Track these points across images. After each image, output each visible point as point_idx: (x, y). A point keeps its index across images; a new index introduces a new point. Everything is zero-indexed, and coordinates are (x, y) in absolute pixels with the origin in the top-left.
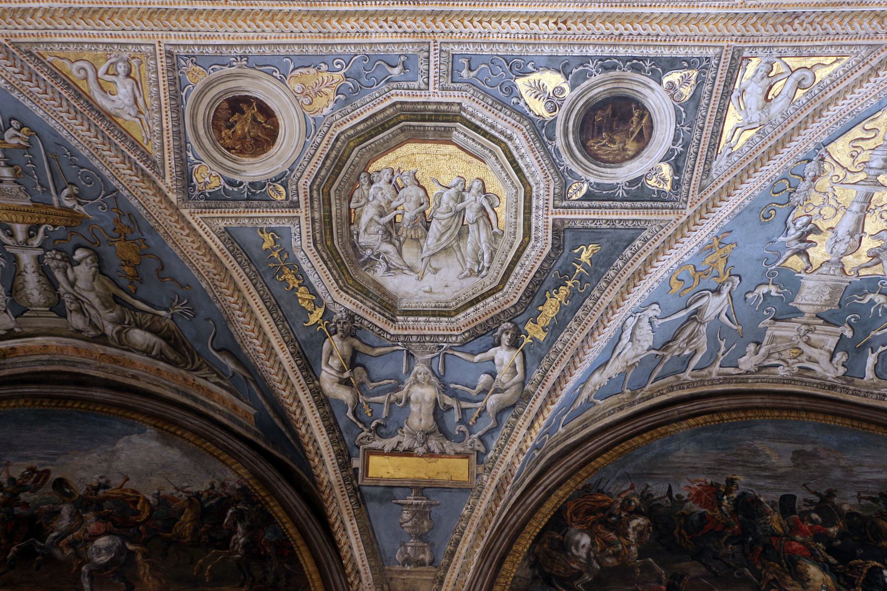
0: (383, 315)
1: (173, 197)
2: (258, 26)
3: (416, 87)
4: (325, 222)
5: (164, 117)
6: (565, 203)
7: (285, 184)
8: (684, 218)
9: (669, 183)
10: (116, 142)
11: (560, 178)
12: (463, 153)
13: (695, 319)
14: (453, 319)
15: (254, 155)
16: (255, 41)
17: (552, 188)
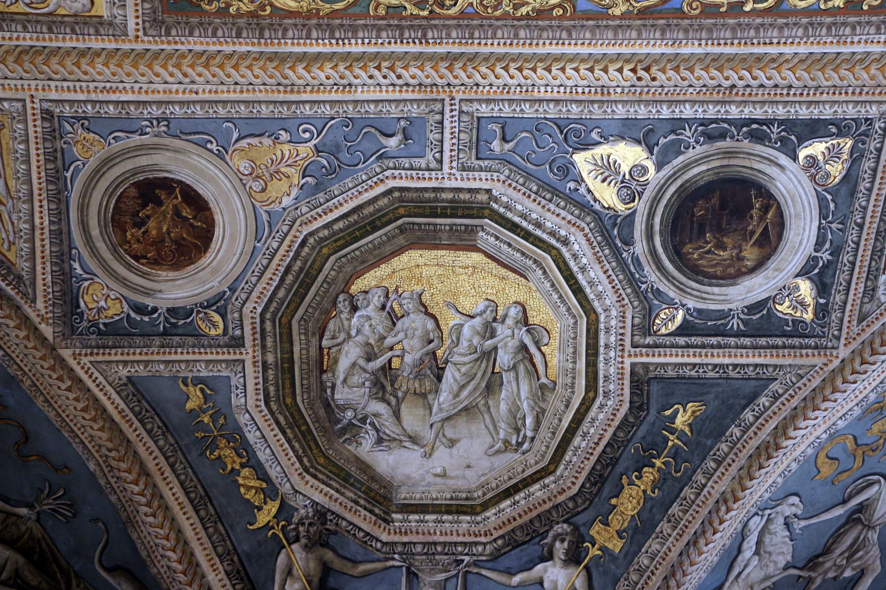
0: (371, 512)
1: (47, 331)
2: (185, 75)
3: (423, 166)
5: (37, 209)
6: (649, 340)
7: (223, 311)
8: (836, 363)
9: (810, 309)
11: (641, 302)
12: (493, 265)
13: (859, 520)
14: (479, 518)
15: (177, 266)
16: (180, 97)
17: (629, 316)
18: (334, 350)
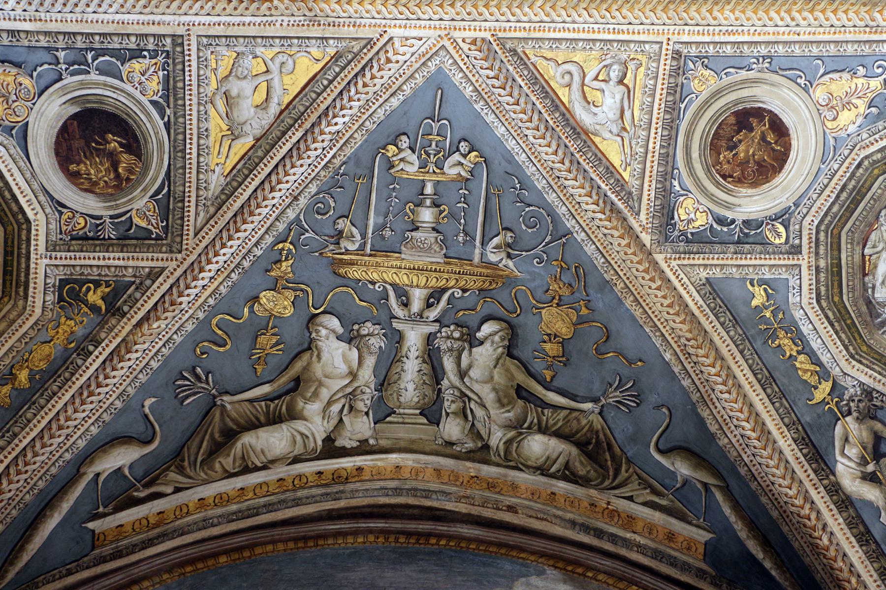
1: (646, 238)
2: (793, 19)
4: (832, 272)
5: (652, 135)
7: (786, 223)
10: (587, 167)
15: (755, 184)
16: (786, 38)
18: (874, 257)
